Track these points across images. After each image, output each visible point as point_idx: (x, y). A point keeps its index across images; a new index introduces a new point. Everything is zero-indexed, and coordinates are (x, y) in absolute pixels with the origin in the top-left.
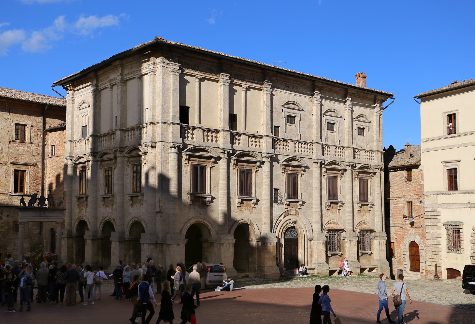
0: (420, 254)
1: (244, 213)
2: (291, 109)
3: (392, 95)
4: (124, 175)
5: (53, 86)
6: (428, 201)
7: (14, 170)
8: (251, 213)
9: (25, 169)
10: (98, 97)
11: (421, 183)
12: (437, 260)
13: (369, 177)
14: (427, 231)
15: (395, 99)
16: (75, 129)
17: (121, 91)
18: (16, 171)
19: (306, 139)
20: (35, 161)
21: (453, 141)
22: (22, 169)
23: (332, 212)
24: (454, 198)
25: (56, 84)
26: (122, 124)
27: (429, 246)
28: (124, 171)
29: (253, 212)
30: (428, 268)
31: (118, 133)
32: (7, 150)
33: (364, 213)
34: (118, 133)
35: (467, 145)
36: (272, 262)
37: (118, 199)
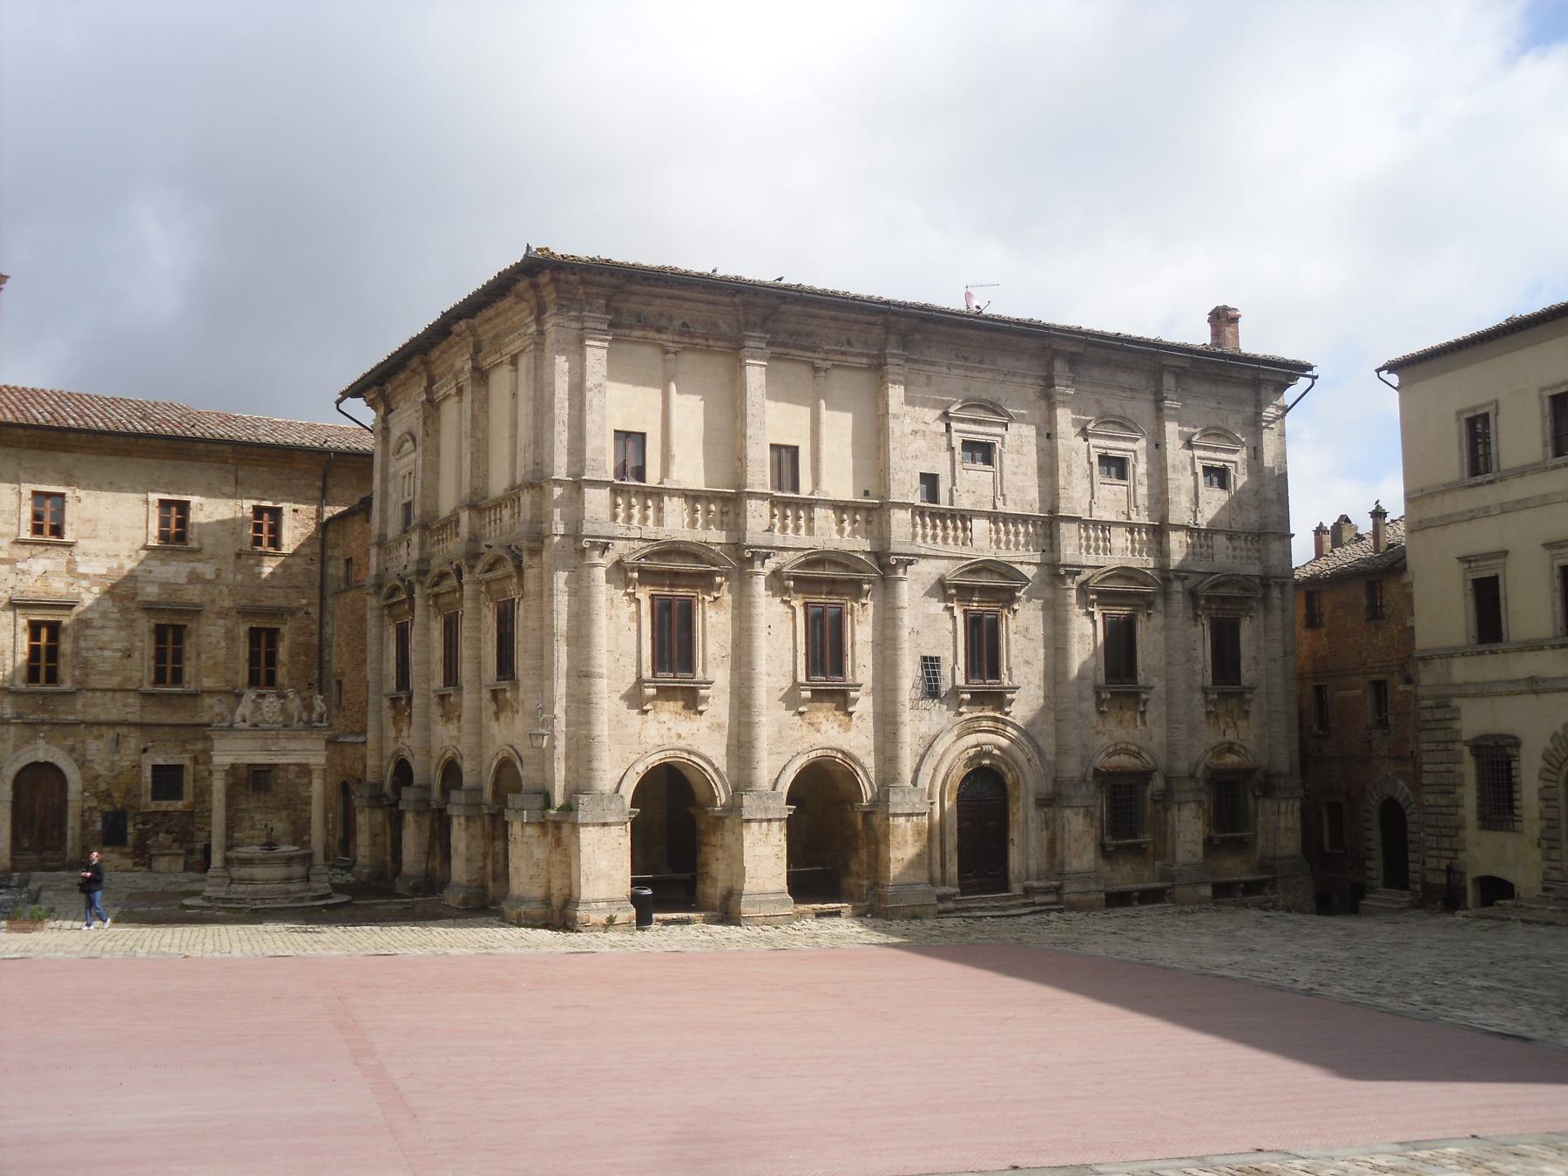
0: (1410, 837)
2: (974, 421)
3: (1310, 368)
4: (480, 631)
5: (338, 402)
6: (1428, 678)
7: (247, 629)
8: (847, 730)
9: (276, 626)
10: (433, 422)
11: (1409, 625)
12: (1451, 854)
13: (1243, 613)
14: (1426, 767)
15: (1317, 377)
16: (390, 511)
17: (472, 401)
18: (254, 634)
19: (1028, 507)
20: (304, 601)
21: (1488, 496)
22: (268, 626)
23: (1121, 721)
24: (1491, 668)
25: (346, 394)
26: (474, 491)
27: (1430, 810)
28: (479, 620)
29: (854, 729)
30: (1430, 878)
31: (465, 516)
32: (231, 577)
33: (1228, 720)
34: (465, 516)
35: (1521, 505)
37: (468, 699)
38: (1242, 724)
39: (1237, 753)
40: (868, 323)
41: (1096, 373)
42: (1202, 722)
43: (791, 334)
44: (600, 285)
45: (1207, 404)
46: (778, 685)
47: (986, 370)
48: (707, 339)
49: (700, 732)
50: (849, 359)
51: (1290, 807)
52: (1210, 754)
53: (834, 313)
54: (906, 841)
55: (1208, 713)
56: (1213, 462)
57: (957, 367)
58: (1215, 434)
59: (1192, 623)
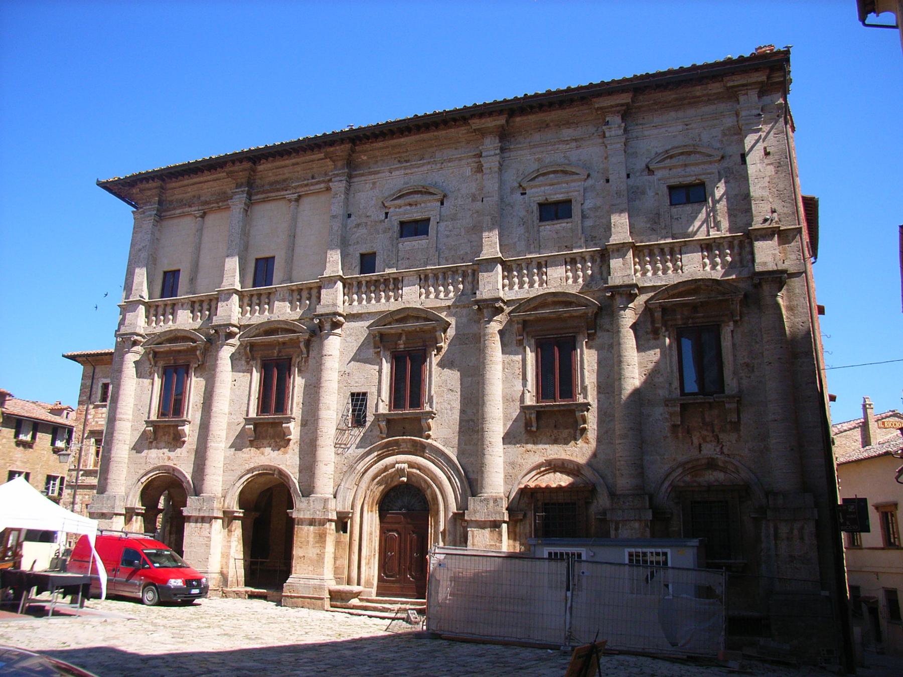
1: (266, 454)
33: (705, 433)
36: (311, 568)
38: (728, 438)
39: (724, 470)
40: (318, 160)
41: (537, 137)
42: (666, 437)
43: (271, 184)
44: (150, 189)
45: (669, 130)
46: (237, 421)
47: (423, 165)
48: (217, 203)
49: (182, 455)
50: (312, 188)
51: (796, 532)
52: (680, 470)
53: (294, 161)
54: (308, 542)
55: (674, 427)
56: (681, 180)
57: (397, 169)
58: (682, 154)
59: (651, 336)
